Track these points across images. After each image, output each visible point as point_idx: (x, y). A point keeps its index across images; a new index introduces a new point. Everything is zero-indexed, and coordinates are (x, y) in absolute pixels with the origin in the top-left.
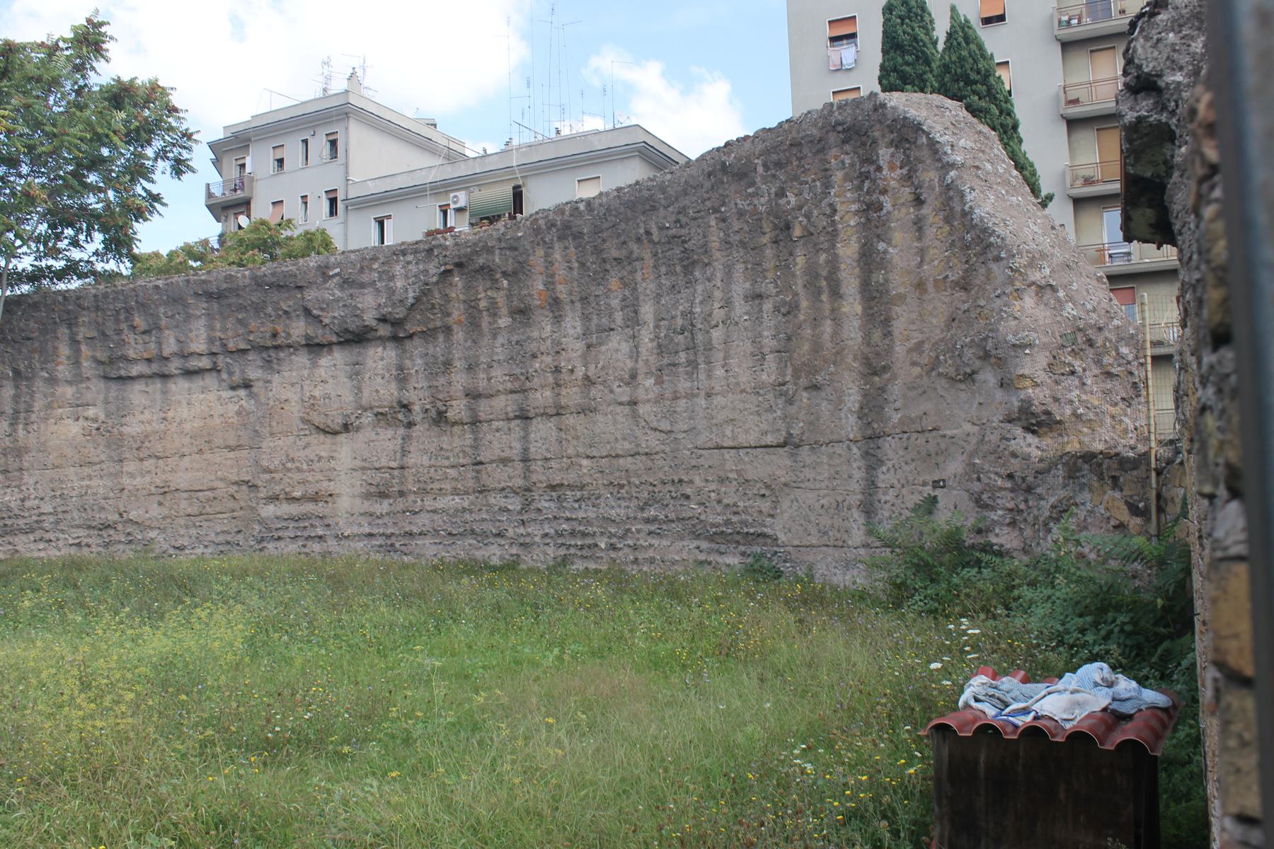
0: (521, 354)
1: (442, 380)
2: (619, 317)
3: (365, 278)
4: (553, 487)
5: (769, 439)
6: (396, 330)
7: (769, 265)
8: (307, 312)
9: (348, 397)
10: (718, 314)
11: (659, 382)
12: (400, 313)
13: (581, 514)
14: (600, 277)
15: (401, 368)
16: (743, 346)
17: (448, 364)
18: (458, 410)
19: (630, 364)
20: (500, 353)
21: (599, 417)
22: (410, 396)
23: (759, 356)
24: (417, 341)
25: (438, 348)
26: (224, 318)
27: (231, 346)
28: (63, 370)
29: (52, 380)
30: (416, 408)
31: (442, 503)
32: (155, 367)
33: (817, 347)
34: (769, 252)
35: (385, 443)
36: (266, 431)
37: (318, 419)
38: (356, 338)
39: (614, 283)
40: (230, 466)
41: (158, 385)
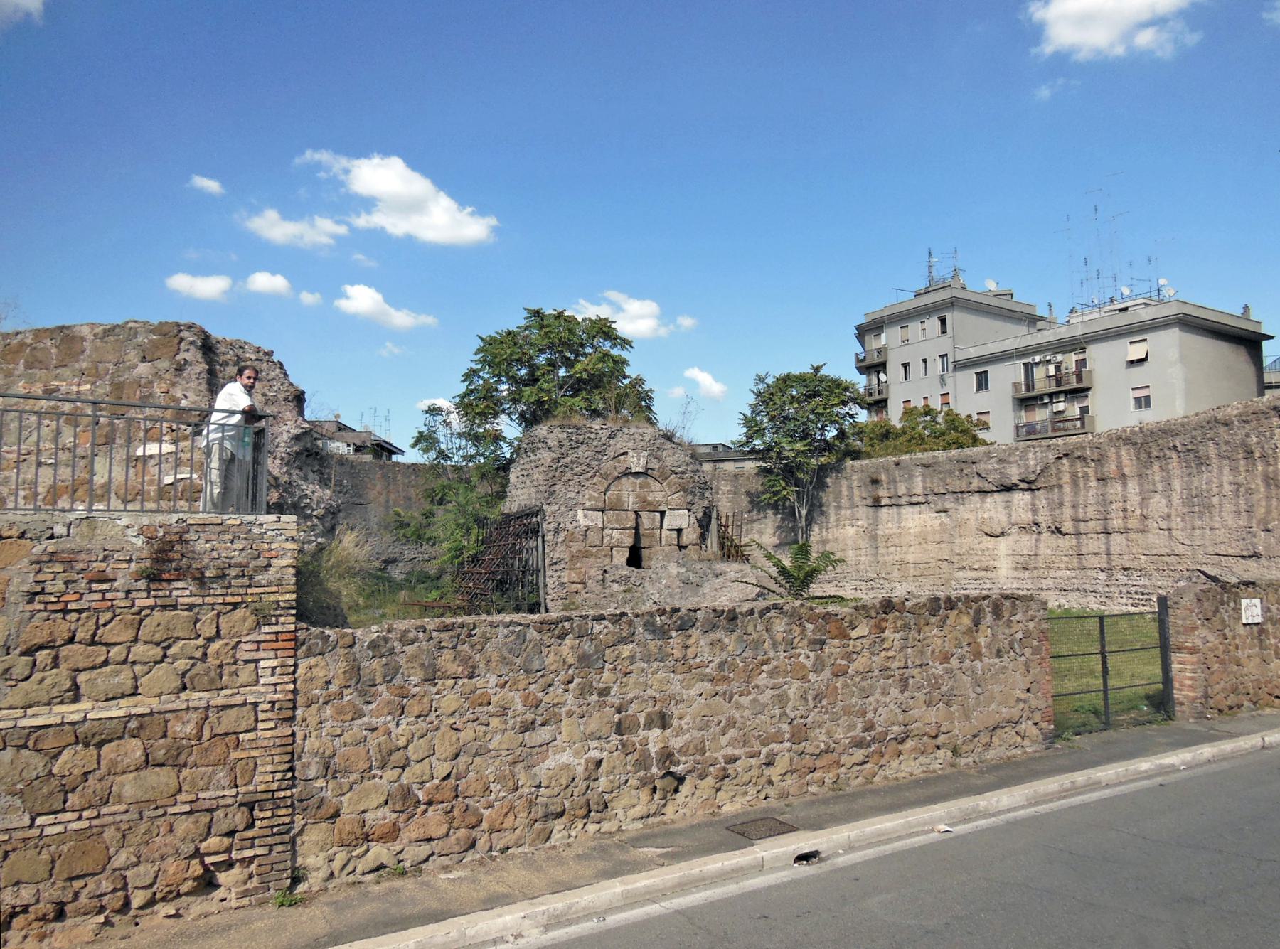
0: (1105, 502)
1: (1058, 512)
2: (1160, 487)
3: (1012, 459)
4: (1125, 569)
5: (1245, 553)
6: (1030, 485)
7: (1242, 469)
8: (979, 475)
9: (1004, 519)
10: (1215, 490)
11: (1183, 520)
12: (1032, 477)
13: (1141, 583)
14: (1148, 465)
15: (1033, 505)
16: (1228, 507)
17: (1061, 504)
18: (1068, 527)
19: (1166, 510)
20: (1091, 500)
21: (1150, 535)
22: (1040, 519)
23: (1238, 513)
24: (1041, 491)
25: (1055, 495)
26: (932, 477)
27: (936, 491)
28: (844, 502)
29: (839, 507)
30: (1043, 525)
31: (1059, 573)
32: (893, 501)
33: (1269, 512)
34: (1242, 462)
35: (1027, 541)
36: (956, 535)
37: (987, 530)
38: (1009, 489)
39: (1156, 468)
40: (934, 551)
41: (895, 509)
